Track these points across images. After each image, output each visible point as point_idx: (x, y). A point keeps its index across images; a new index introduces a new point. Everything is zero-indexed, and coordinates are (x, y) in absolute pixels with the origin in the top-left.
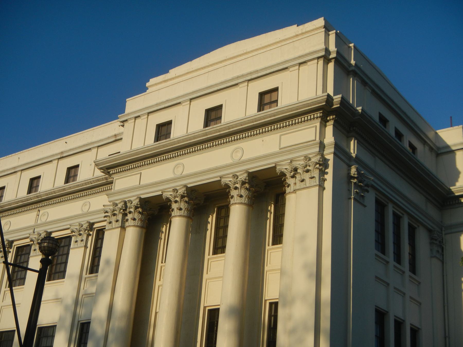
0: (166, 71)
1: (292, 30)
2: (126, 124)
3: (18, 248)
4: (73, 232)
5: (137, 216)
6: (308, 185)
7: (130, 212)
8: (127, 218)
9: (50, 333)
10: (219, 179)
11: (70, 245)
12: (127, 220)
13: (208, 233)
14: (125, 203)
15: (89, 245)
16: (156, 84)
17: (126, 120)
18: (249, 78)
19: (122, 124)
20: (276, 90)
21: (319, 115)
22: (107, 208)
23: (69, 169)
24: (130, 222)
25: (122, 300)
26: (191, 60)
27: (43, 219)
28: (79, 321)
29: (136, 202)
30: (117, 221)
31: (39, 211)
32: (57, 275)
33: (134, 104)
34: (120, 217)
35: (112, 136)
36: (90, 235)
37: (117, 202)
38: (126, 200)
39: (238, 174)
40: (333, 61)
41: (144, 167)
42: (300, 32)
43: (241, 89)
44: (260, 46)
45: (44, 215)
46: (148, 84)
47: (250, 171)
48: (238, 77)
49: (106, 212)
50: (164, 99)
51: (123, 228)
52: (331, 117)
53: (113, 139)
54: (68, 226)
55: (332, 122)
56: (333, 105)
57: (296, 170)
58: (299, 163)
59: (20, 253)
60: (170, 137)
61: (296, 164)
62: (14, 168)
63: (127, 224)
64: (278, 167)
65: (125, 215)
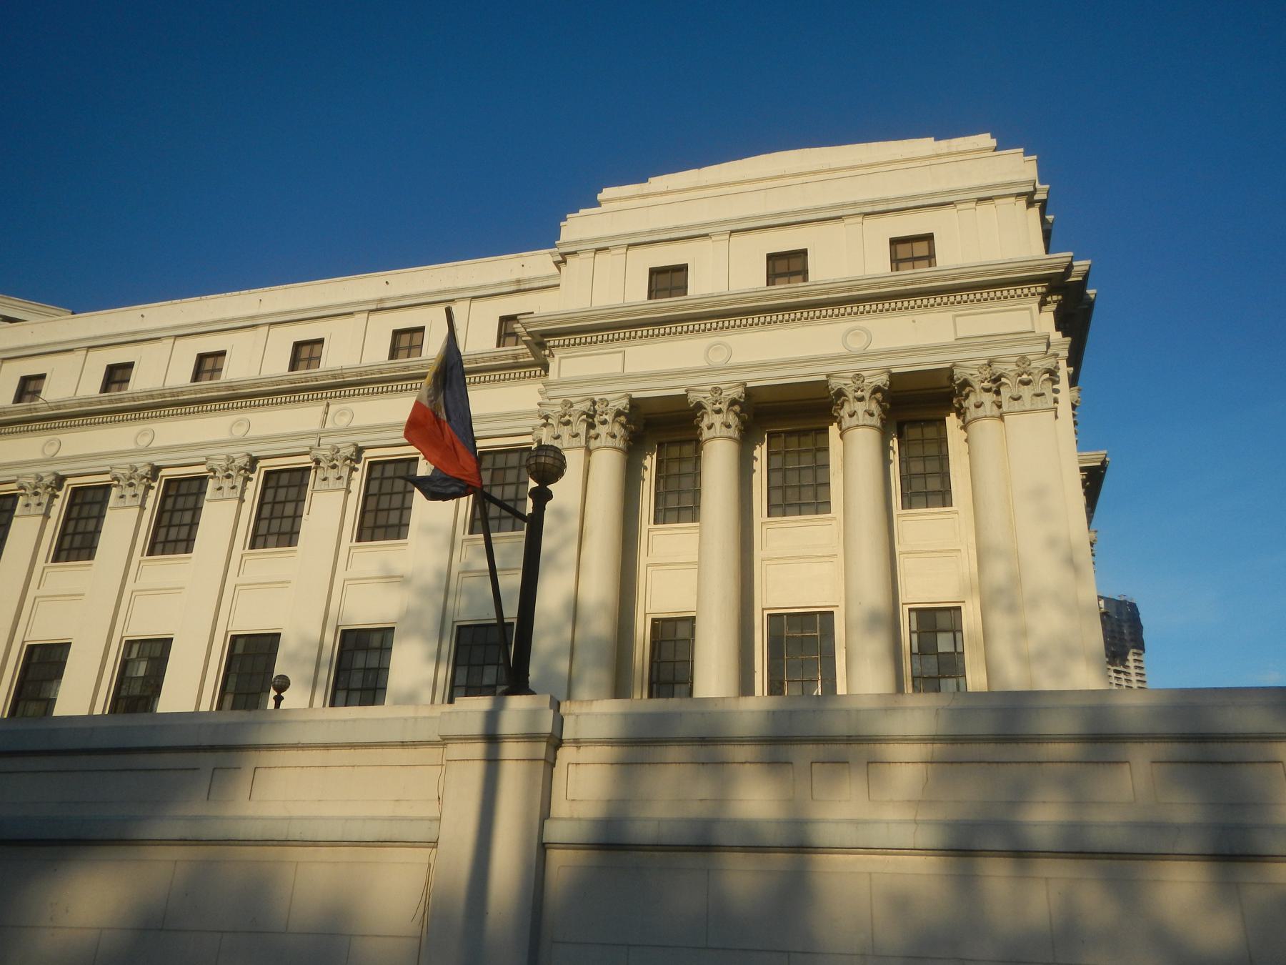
0: (643, 179)
1: (925, 146)
2: (569, 259)
3: (267, 473)
4: (21, 488)
5: (617, 430)
6: (1028, 407)
7: (604, 422)
8: (592, 432)
9: (376, 641)
10: (824, 378)
11: (13, 510)
12: (597, 437)
13: (756, 477)
14: (594, 403)
16: (620, 199)
17: (575, 253)
18: (868, 209)
19: (560, 259)
20: (929, 238)
21: (1040, 290)
22: (548, 410)
24: (604, 440)
25: (597, 588)
26: (699, 164)
27: (342, 422)
28: (23, 643)
29: (623, 404)
30: (576, 435)
31: (328, 405)
32: (379, 532)
33: (576, 227)
35: (510, 283)
37: (572, 400)
38: (596, 398)
39: (864, 374)
40: (1038, 205)
41: (632, 342)
42: (945, 151)
43: (851, 228)
44: (859, 163)
46: (600, 197)
47: (894, 371)
48: (844, 205)
49: (547, 417)
50: (671, 224)
51: (589, 452)
52: (1055, 298)
53: (514, 288)
54: (108, 469)
55: (1054, 307)
56: (1069, 276)
57: (997, 380)
58: (1009, 368)
59: (78, 501)
60: (686, 294)
61: (998, 368)
63: (593, 444)
64: (957, 371)
65: (591, 426)
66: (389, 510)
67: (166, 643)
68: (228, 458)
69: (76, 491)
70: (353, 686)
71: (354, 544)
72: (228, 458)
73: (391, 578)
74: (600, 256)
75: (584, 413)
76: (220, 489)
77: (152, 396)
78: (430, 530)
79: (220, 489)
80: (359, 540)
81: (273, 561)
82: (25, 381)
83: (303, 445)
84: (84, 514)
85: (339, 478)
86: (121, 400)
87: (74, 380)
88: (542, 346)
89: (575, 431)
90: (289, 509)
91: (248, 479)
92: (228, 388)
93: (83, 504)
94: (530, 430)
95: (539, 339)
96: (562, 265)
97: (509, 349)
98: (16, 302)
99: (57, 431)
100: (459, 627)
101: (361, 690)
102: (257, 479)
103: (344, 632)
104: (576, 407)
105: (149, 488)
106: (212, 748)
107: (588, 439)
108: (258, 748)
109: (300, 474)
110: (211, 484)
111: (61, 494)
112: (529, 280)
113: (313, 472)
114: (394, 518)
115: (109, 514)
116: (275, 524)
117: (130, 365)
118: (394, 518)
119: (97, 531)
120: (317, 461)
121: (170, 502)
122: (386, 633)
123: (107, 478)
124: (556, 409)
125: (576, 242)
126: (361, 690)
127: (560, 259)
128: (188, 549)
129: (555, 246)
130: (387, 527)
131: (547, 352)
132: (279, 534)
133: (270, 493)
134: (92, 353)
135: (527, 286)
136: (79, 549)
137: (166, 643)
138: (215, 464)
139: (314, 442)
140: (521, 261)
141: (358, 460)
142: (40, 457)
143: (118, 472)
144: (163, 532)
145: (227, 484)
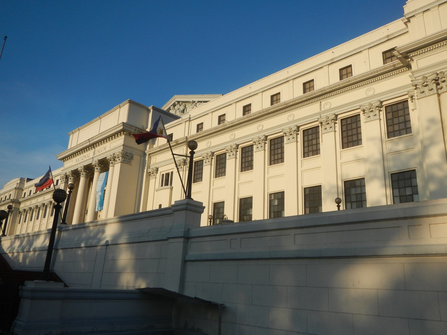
2: (411, 20)
8: (438, 87)
9: (358, 183)
14: (437, 74)
15: (382, 117)
19: (407, 20)
22: (416, 82)
23: (272, 97)
27: (327, 107)
30: (432, 89)
31: (321, 102)
34: (434, 86)
36: (381, 111)
38: (438, 72)
45: (326, 104)
49: (416, 85)
51: (439, 95)
62: (287, 78)
63: (440, 91)
65: (438, 84)
66: (352, 135)
67: (282, 193)
68: (290, 128)
69: (243, 149)
70: (353, 201)
71: (342, 150)
72: (290, 128)
73: (359, 160)
74: (425, 14)
75: (434, 80)
76: (289, 139)
77: (260, 113)
78: (372, 139)
79: (289, 139)
80: (343, 148)
81: (312, 161)
82: (245, 107)
83: (315, 118)
84: (247, 155)
85: (331, 127)
86: (251, 116)
87: (234, 114)
88: (407, 57)
89: (430, 88)
90: (314, 142)
91: (297, 134)
92: (285, 104)
93: (245, 152)
94: (407, 93)
95: (405, 55)
96: (409, 24)
97: (390, 64)
98: (206, 96)
99: (233, 131)
100: (391, 174)
101: (356, 202)
102: (301, 133)
103: (345, 182)
104: (428, 78)
105: (265, 143)
106: (405, 218)
107: (437, 90)
108: (428, 216)
109: (315, 129)
110: (285, 139)
111: (238, 150)
112: (392, 34)
113: (320, 127)
114: (355, 138)
115: (255, 154)
116: (310, 148)
117: (250, 105)
118: (355, 138)
119: (252, 160)
120: (321, 123)
121: (273, 147)
122: (362, 180)
123: (252, 142)
124: (419, 81)
125: (413, 11)
126: (356, 202)
127: (407, 20)
128: (282, 161)
129: (404, 16)
130: (353, 141)
131: (409, 60)
132: (313, 151)
133: (306, 138)
134: (238, 104)
135: (392, 37)
136: (278, 159)
137: (282, 193)
138: (285, 131)
139: (319, 116)
140: (387, 28)
141: (336, 120)
142: (230, 140)
143: (255, 140)
144: (272, 157)
145: (291, 137)
